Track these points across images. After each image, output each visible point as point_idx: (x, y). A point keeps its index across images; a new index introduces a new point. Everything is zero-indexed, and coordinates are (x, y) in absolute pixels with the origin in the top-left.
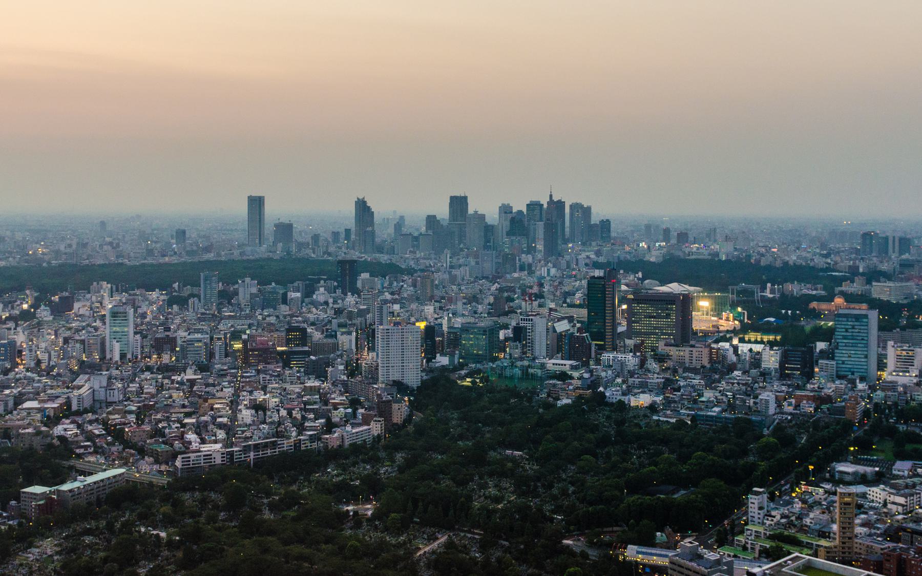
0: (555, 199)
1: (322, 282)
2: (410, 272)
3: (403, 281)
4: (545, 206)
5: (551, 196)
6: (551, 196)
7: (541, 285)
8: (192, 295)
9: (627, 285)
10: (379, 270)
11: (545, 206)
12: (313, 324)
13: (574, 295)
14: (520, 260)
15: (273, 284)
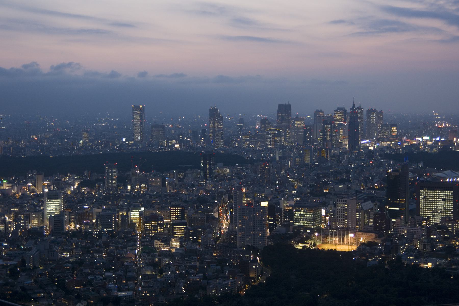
0: (356, 106)
1: (189, 169)
2: (252, 161)
3: (247, 169)
4: (349, 111)
5: (354, 105)
6: (354, 105)
7: (348, 172)
8: (98, 181)
9: (412, 172)
10: (229, 160)
11: (349, 111)
12: (186, 202)
13: (372, 179)
14: (331, 152)
15: (155, 171)
